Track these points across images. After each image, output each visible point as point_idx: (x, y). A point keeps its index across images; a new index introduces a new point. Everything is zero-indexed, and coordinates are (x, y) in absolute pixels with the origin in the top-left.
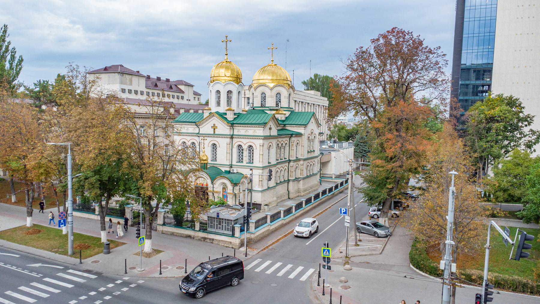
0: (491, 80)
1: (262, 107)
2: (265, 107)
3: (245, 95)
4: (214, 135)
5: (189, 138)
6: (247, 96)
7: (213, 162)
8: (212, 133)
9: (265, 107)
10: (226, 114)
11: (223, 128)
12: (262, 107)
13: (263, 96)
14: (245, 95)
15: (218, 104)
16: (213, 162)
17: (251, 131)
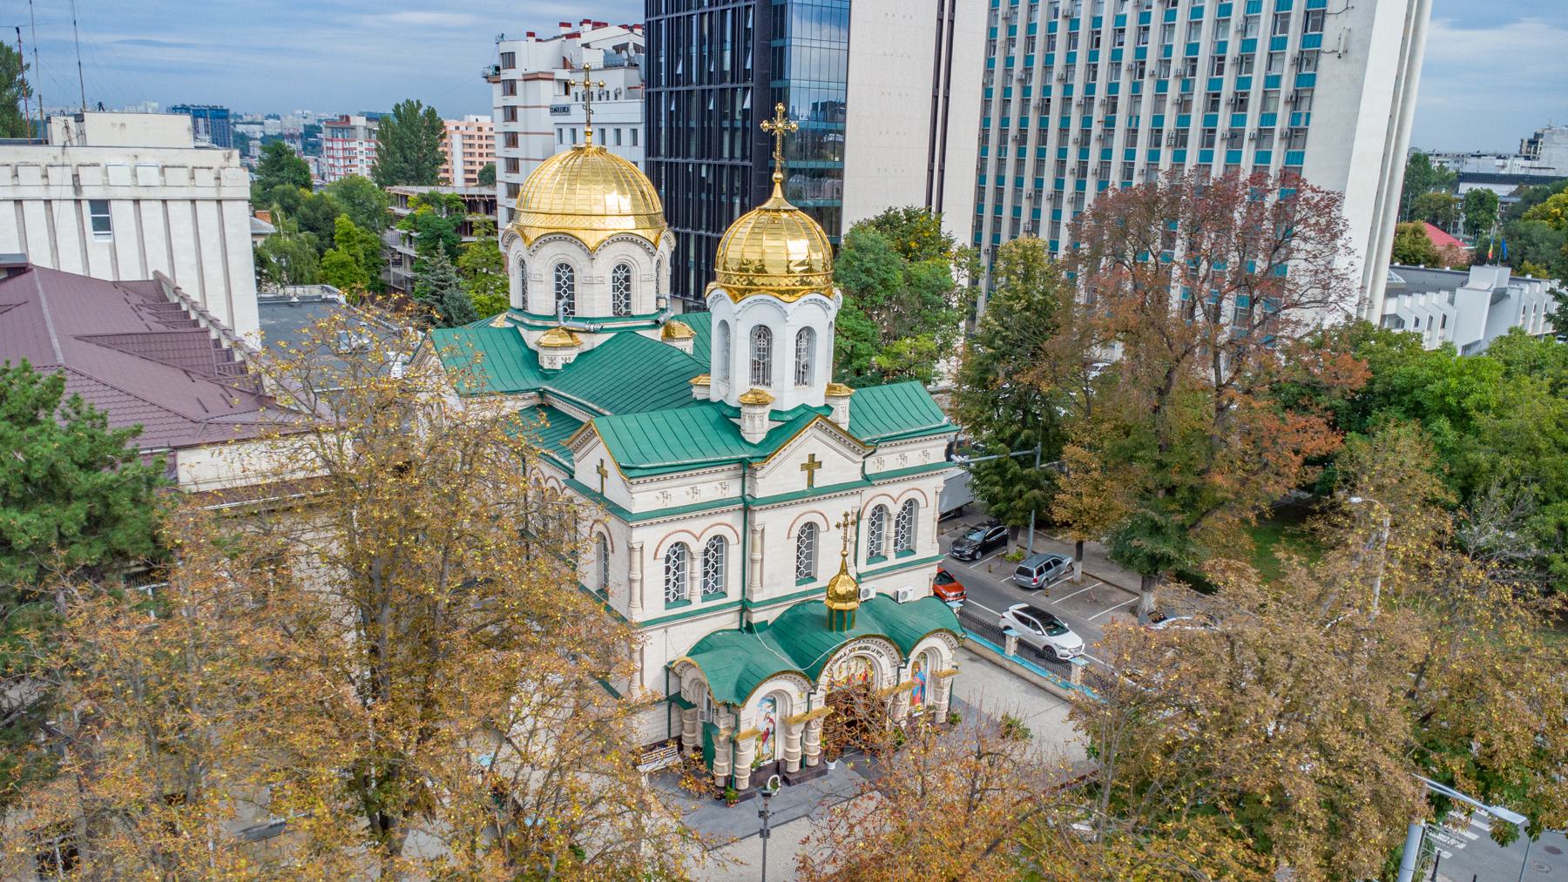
0: (842, 160)
1: (617, 316)
2: (629, 316)
3: (77, 187)
4: (814, 493)
5: (697, 525)
6: (90, 193)
7: (803, 588)
8: (803, 486)
9: (629, 316)
10: (828, 408)
11: (839, 466)
12: (617, 316)
13: (622, 274)
14: (77, 187)
15: (802, 374)
16: (803, 588)
17: (914, 455)
